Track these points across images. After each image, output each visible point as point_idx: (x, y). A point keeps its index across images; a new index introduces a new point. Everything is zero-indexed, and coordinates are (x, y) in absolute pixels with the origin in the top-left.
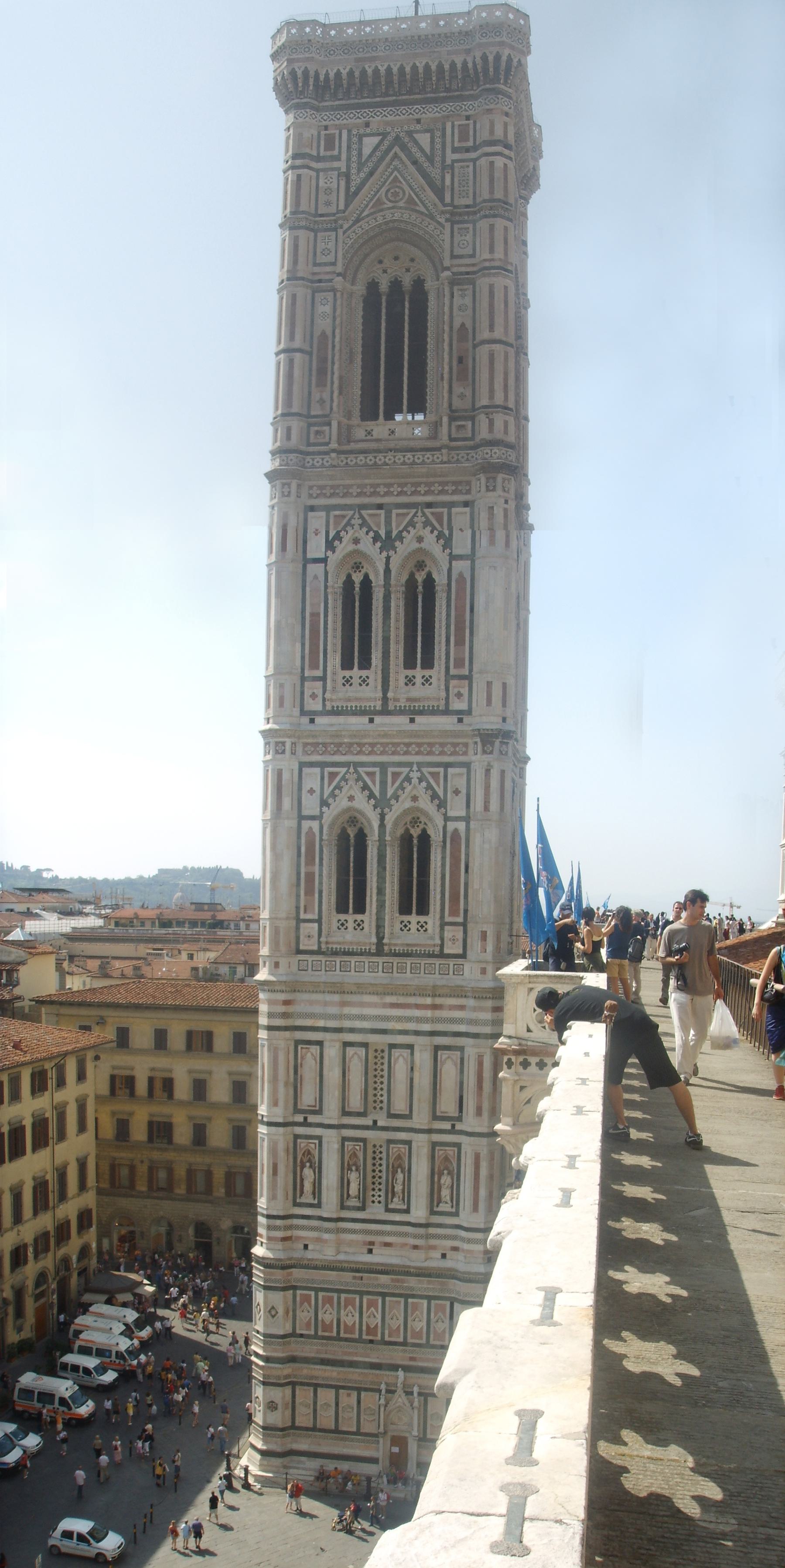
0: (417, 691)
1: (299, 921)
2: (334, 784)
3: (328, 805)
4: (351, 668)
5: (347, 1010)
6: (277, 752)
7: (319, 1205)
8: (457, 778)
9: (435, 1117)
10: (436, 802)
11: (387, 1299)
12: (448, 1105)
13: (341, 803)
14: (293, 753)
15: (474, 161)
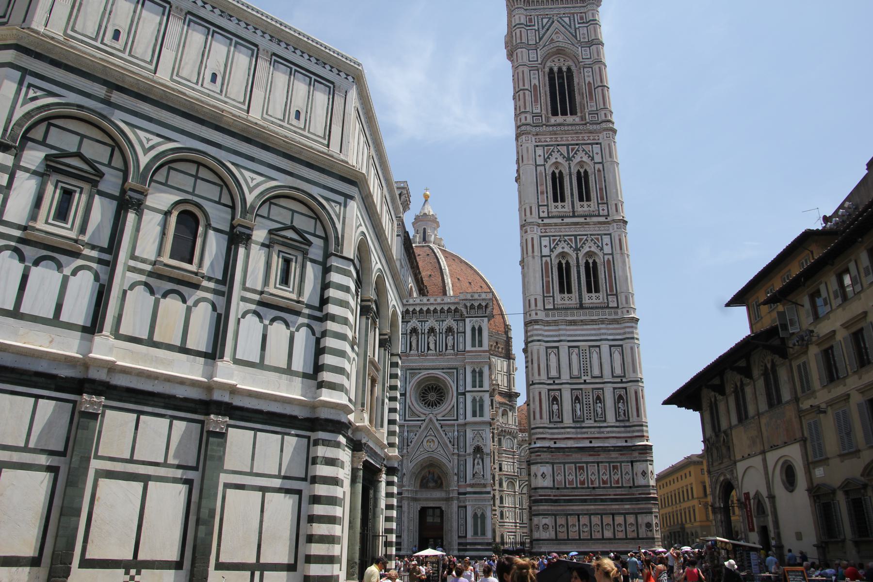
0: (586, 209)
1: (544, 297)
2: (555, 243)
3: (553, 252)
4: (558, 202)
5: (568, 333)
6: (531, 231)
7: (562, 422)
8: (606, 239)
9: (613, 377)
10: (600, 248)
11: (600, 464)
12: (618, 371)
13: (559, 250)
14: (537, 231)
15: (587, 27)
